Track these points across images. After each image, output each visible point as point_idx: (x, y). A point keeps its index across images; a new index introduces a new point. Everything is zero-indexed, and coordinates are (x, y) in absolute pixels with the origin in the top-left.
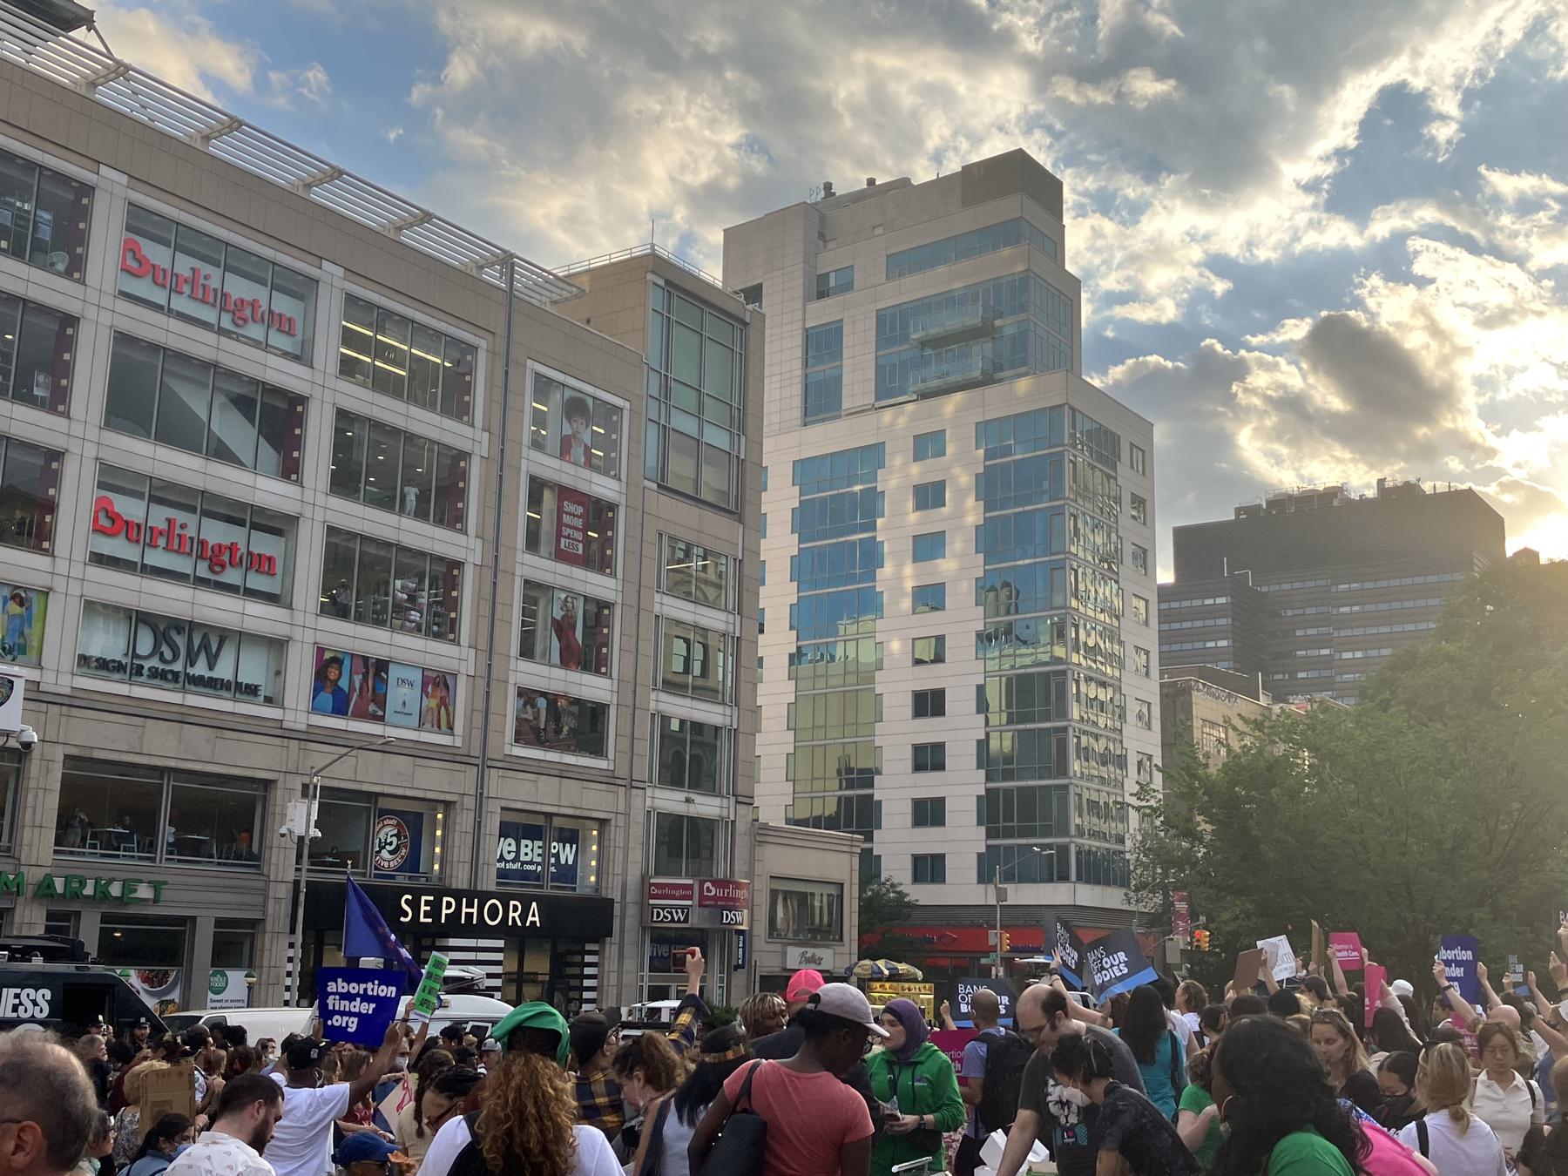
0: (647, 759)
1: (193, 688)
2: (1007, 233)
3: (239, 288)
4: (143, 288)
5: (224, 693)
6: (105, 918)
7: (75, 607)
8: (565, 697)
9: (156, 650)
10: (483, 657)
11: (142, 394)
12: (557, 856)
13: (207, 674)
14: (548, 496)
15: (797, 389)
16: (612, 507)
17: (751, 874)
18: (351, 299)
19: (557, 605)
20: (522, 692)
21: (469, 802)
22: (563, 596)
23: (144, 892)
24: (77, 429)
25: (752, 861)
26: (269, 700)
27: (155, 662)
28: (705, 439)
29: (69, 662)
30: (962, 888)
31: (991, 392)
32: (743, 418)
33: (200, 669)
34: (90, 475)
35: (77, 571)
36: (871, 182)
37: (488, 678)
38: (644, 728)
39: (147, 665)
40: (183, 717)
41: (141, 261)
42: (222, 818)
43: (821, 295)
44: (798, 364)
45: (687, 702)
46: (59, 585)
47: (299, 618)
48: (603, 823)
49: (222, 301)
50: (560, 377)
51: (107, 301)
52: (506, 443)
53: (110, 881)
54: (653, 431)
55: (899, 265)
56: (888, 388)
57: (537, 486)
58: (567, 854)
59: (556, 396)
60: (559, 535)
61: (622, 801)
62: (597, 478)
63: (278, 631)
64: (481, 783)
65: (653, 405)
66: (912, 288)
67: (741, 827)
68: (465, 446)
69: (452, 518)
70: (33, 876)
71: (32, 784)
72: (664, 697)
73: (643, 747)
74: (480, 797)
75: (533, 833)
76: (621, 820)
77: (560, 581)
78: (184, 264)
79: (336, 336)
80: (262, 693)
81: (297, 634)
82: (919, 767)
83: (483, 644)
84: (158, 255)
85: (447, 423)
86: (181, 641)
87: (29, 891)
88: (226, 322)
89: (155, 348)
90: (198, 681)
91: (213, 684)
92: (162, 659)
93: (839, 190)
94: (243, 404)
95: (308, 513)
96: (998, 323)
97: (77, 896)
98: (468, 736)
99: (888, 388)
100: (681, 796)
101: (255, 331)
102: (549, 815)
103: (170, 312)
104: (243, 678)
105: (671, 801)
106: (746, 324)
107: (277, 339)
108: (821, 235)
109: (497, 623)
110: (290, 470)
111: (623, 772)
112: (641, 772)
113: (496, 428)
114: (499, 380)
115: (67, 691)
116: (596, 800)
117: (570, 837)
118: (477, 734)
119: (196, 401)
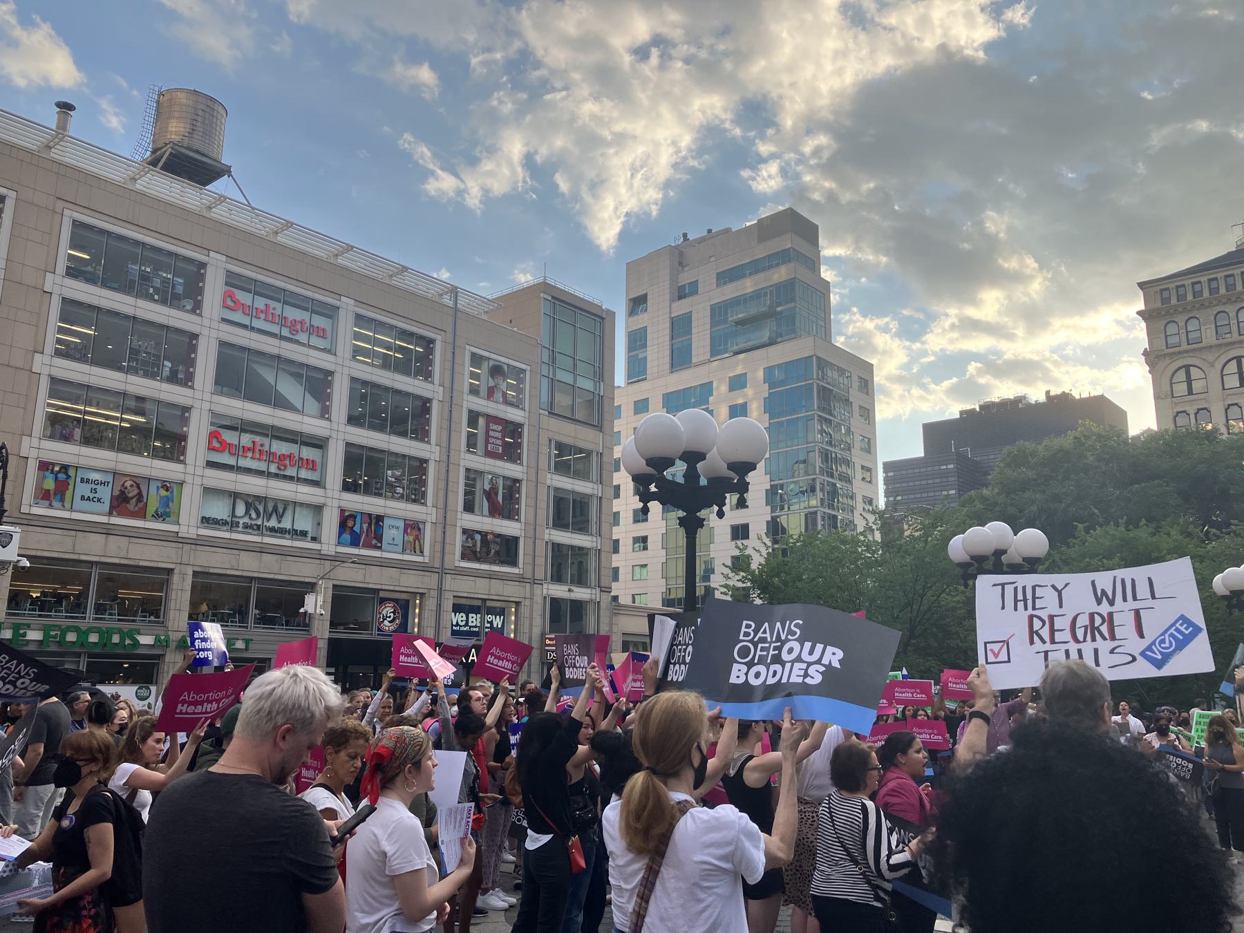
0: (543, 566)
2: (783, 257)
3: (293, 314)
4: (238, 317)
7: (198, 491)
8: (492, 533)
10: (441, 512)
11: (236, 373)
12: (491, 623)
13: (277, 525)
14: (481, 421)
15: (667, 353)
16: (521, 425)
18: (359, 317)
19: (486, 482)
20: (465, 531)
21: (434, 593)
24: (198, 395)
25: (611, 625)
26: (314, 539)
27: (246, 520)
29: (195, 519)
31: (772, 350)
32: (602, 371)
33: (273, 523)
35: (199, 471)
36: (710, 231)
37: (444, 524)
38: (541, 550)
40: (262, 550)
41: (235, 301)
43: (680, 298)
44: (668, 338)
45: (569, 535)
46: (189, 479)
47: (330, 493)
48: (518, 604)
49: (283, 321)
50: (486, 354)
51: (215, 325)
52: (449, 391)
54: (545, 382)
55: (725, 277)
56: (717, 348)
57: (473, 418)
58: (497, 622)
59: (485, 365)
60: (487, 442)
62: (510, 409)
64: (441, 582)
65: (545, 367)
66: (731, 291)
67: (603, 605)
68: (428, 395)
69: (421, 434)
70: (175, 637)
71: (175, 587)
72: (554, 532)
73: (540, 561)
75: (475, 610)
76: (527, 602)
77: (487, 468)
78: (260, 303)
79: (349, 335)
80: (310, 535)
81: (329, 502)
83: (441, 505)
84: (244, 297)
87: (173, 645)
88: (285, 332)
89: (243, 349)
90: (272, 530)
91: (283, 531)
92: (251, 518)
93: (691, 237)
94: (297, 376)
95: (334, 436)
96: (779, 309)
98: (432, 557)
99: (717, 348)
100: (566, 588)
101: (303, 337)
102: (484, 600)
103: (252, 329)
105: (559, 591)
106: (603, 319)
107: (315, 341)
108: (680, 264)
109: (450, 494)
110: (325, 413)
112: (540, 574)
113: (447, 384)
114: (449, 357)
116: (512, 591)
117: (501, 612)
118: (438, 555)
119: (269, 375)
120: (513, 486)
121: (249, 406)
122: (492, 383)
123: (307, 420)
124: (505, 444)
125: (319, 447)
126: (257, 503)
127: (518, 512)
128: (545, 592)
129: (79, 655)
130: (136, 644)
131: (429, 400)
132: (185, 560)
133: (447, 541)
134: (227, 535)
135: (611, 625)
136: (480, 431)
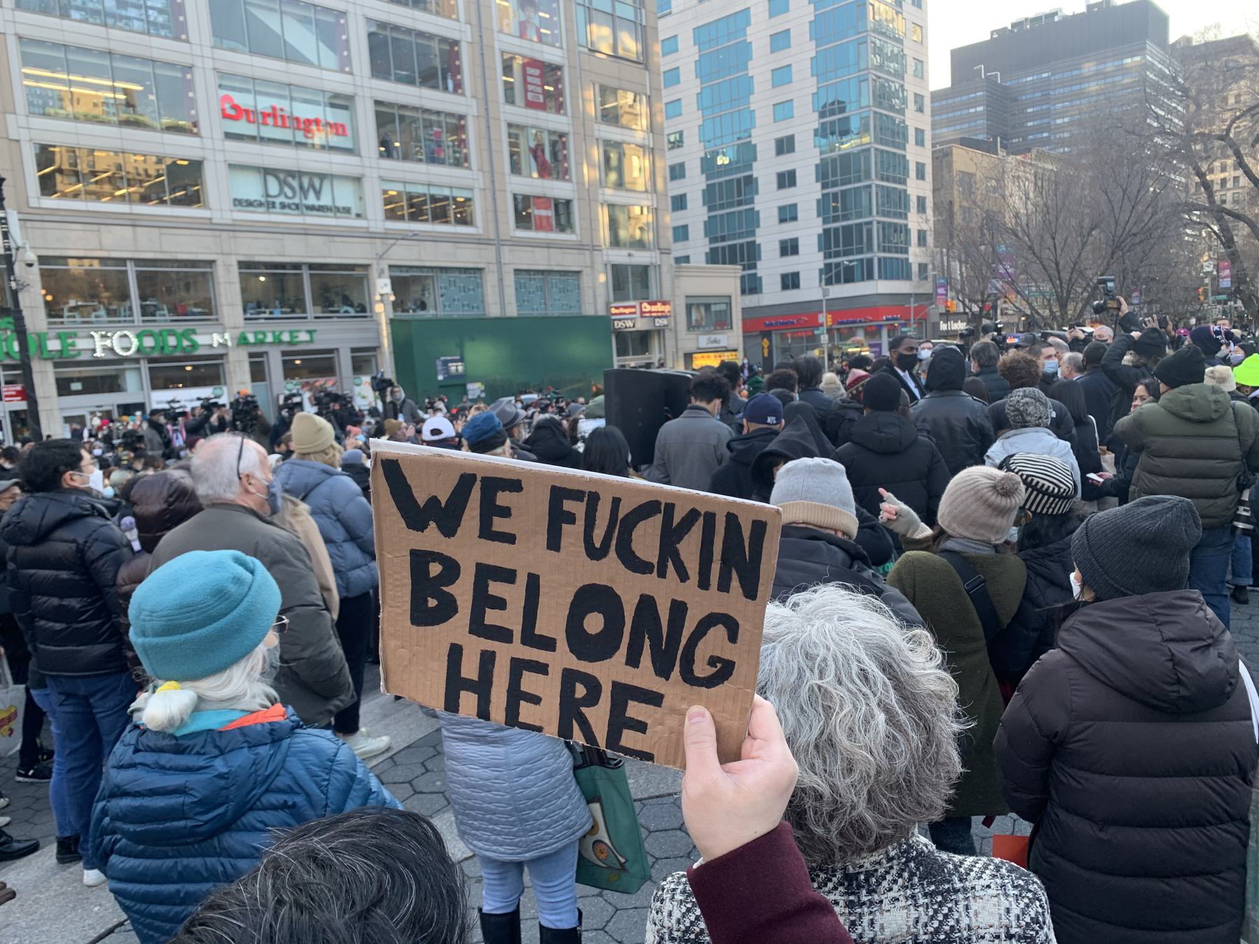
1: (309, 212)
5: (330, 214)
6: (284, 353)
7: (223, 168)
9: (281, 192)
10: (488, 175)
13: (316, 203)
17: (673, 294)
19: (531, 138)
21: (494, 268)
22: (534, 131)
23: (304, 337)
25: (673, 288)
26: (358, 216)
27: (282, 199)
28: (618, 14)
29: (228, 204)
30: (811, 289)
33: (312, 200)
34: (212, 80)
39: (278, 201)
40: (306, 232)
42: (338, 289)
47: (366, 162)
53: (281, 333)
60: (526, 91)
61: (588, 258)
62: (546, 48)
63: (355, 171)
67: (664, 269)
71: (221, 280)
74: (499, 263)
77: (531, 122)
80: (354, 211)
82: (782, 220)
83: (487, 168)
85: (440, 20)
86: (295, 183)
90: (311, 208)
91: (321, 208)
92: (286, 197)
97: (262, 343)
104: (340, 204)
109: (494, 154)
111: (587, 241)
115: (230, 222)
118: (492, 225)
120: (559, 141)
121: (258, 61)
122: (523, 18)
123: (326, 75)
124: (547, 94)
125: (345, 108)
126: (290, 180)
127: (566, 171)
128: (605, 258)
129: (137, 361)
130: (194, 345)
131: (456, 43)
132: (226, 250)
133: (499, 208)
134: (265, 217)
135: (673, 288)
136: (516, 79)
